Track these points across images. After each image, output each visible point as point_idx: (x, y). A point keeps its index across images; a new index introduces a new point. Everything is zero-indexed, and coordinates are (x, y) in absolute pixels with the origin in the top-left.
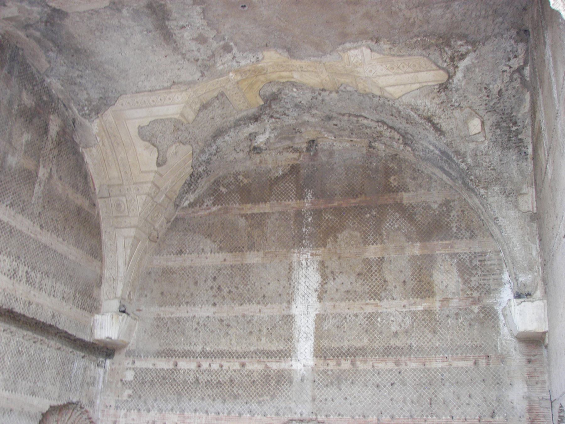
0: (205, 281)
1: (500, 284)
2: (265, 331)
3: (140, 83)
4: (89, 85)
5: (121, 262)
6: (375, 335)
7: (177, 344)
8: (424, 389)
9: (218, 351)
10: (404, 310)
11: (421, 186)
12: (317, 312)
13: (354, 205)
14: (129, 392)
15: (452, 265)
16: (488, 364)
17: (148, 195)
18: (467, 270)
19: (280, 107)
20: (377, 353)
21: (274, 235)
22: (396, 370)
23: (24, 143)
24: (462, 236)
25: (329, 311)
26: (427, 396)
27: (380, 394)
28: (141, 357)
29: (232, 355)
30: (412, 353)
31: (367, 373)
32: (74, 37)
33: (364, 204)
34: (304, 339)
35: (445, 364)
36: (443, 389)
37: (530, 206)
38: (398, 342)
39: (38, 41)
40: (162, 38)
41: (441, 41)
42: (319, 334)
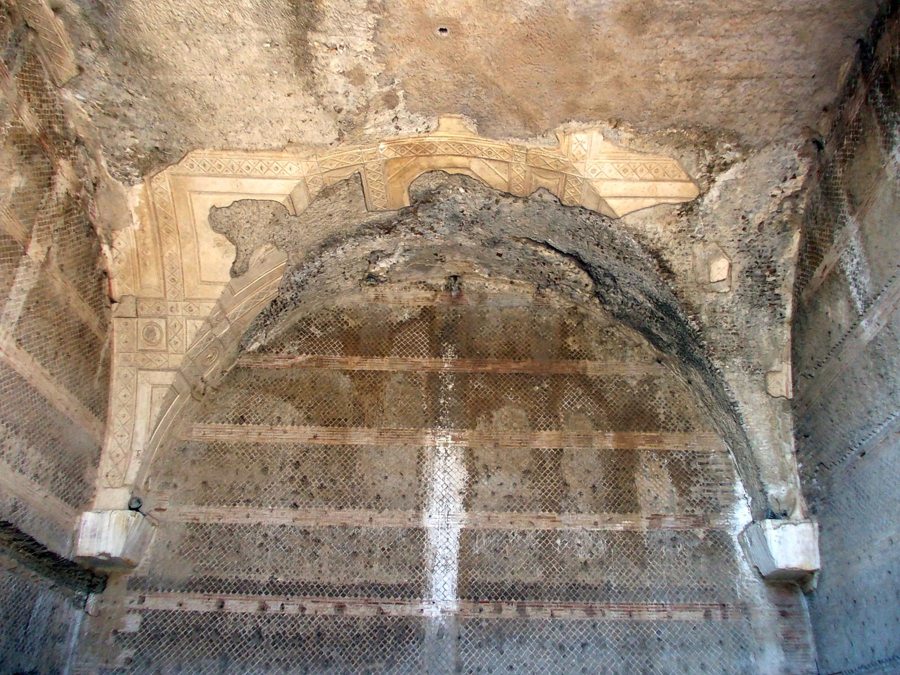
0: (281, 469)
1: (733, 499)
2: (378, 553)
3: (232, 134)
4: (140, 123)
5: (141, 426)
6: (554, 566)
7: (225, 569)
8: (633, 654)
9: (297, 583)
10: (596, 529)
11: (611, 354)
12: (462, 526)
13: (515, 371)
14: (130, 653)
15: (661, 467)
16: (725, 617)
17: (208, 320)
18: (685, 476)
19: (429, 216)
20: (558, 594)
21: (395, 406)
22: (588, 622)
23: (12, 190)
24: (673, 427)
25: (481, 525)
26: (638, 666)
27: (565, 660)
28: (157, 590)
29: (321, 590)
30: (611, 596)
31: (543, 626)
32: (138, 29)
33: (531, 372)
34: (442, 568)
35: (662, 614)
36: (661, 655)
37: (784, 389)
38: (589, 579)
39: (71, 24)
40: (293, 62)
41: (704, 138)
42: (466, 561)
